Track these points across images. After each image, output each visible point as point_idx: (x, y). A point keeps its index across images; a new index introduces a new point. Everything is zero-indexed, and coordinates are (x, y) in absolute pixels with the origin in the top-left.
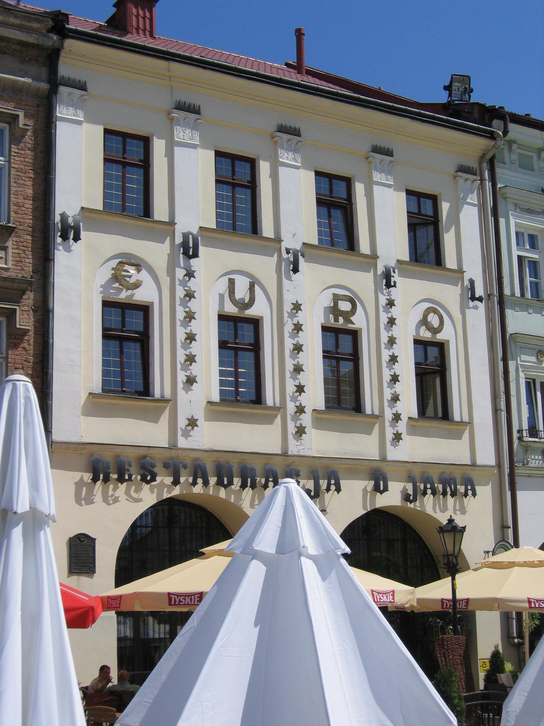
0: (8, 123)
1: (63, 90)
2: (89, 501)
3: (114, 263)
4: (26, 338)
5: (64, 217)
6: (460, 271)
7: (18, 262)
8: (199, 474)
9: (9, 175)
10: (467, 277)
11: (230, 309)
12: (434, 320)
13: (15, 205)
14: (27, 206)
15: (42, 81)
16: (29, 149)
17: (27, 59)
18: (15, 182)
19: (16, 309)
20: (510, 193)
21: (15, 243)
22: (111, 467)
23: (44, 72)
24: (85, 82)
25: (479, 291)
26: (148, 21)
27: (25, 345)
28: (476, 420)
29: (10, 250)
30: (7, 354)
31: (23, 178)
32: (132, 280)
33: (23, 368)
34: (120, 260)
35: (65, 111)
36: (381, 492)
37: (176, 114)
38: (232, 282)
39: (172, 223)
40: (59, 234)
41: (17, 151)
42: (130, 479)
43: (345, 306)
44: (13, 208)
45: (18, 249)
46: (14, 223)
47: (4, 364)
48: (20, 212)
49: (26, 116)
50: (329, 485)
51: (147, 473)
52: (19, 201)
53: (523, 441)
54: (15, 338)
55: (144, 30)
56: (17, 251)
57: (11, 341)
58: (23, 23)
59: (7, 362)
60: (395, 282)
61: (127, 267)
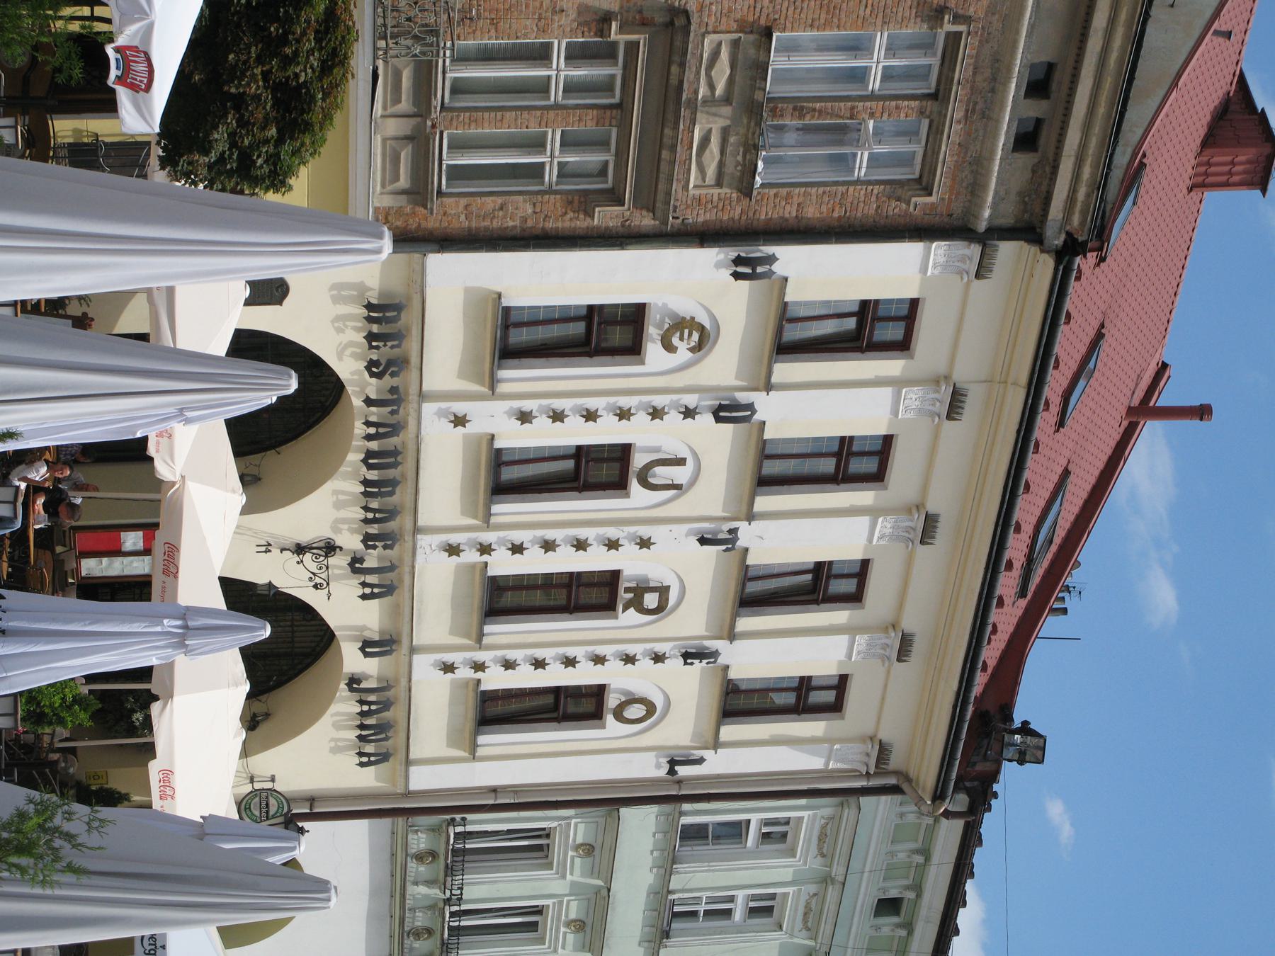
1: (976, 250)
2: (336, 300)
4: (582, 216)
5: (771, 259)
6: (716, 745)
7: (699, 201)
8: (381, 430)
10: (708, 754)
11: (638, 461)
12: (636, 711)
13: (788, 194)
14: (788, 207)
16: (878, 207)
17: (1026, 199)
18: (824, 193)
19: (623, 205)
20: (849, 814)
21: (728, 195)
23: (1007, 221)
25: (682, 771)
26: (1223, 179)
27: (571, 215)
28: (478, 765)
29: (716, 191)
30: (556, 192)
31: (832, 202)
32: (675, 340)
33: (535, 213)
34: (707, 325)
35: (941, 252)
36: (362, 649)
37: (945, 393)
38: (681, 462)
39: (769, 387)
40: (743, 255)
41: (875, 191)
42: (371, 347)
43: (651, 600)
44: (784, 191)
45: (719, 199)
46: (759, 193)
48: (777, 200)
49: (933, 204)
50: (371, 586)
51: (381, 368)
52: (795, 198)
53: (449, 825)
54: (580, 202)
55: (1206, 174)
56: (715, 198)
57: (576, 198)
60: (692, 664)
61: (696, 336)
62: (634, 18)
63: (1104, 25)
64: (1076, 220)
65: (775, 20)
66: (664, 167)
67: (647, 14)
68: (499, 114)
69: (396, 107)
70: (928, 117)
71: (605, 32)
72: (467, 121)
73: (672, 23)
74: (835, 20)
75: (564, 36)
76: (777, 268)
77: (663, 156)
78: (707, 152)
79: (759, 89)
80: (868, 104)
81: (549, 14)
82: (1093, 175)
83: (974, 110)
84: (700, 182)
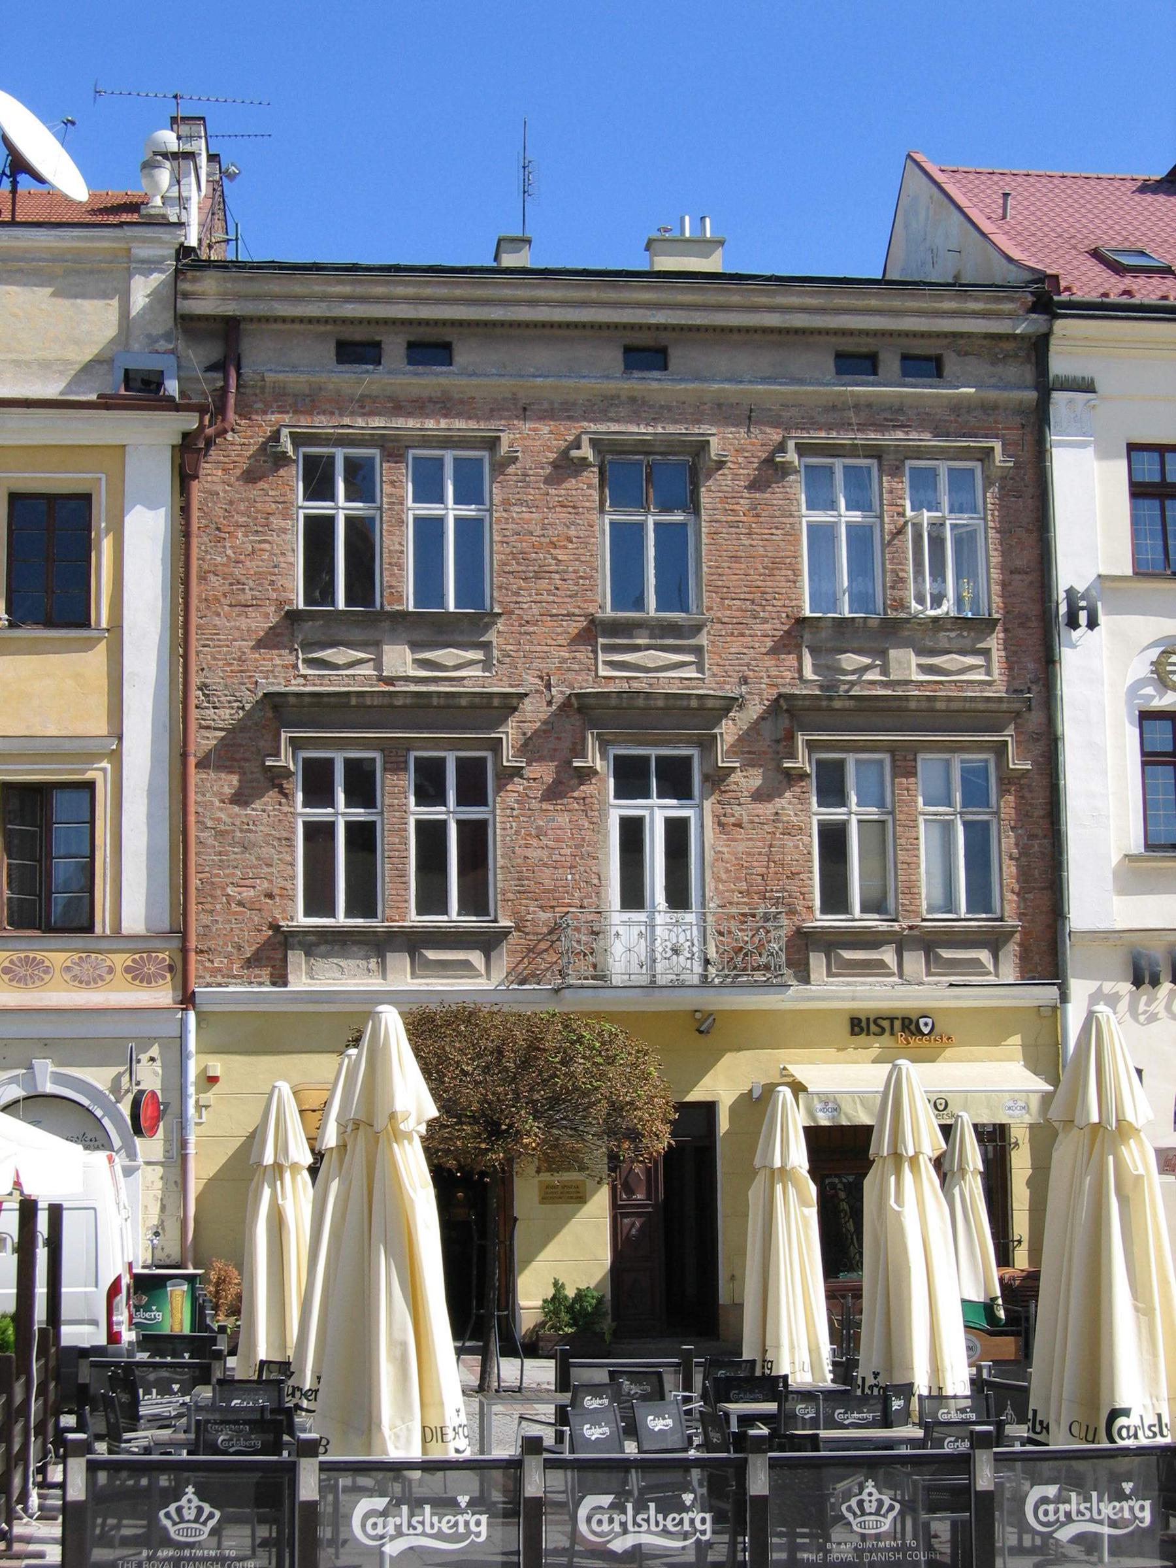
0: (979, 460)
1: (1059, 398)
3: (1154, 654)
5: (1070, 592)
9: (986, 538)
15: (1026, 388)
22: (1161, 963)
23: (1028, 373)
24: (1092, 379)
34: (1162, 648)
47: (995, 821)
58: (988, 306)
59: (999, 819)
62: (785, 747)
63: (778, 315)
64: (1007, 306)
65: (787, 616)
66: (955, 705)
67: (781, 734)
68: (899, 866)
69: (891, 965)
70: (903, 462)
71: (800, 772)
72: (908, 896)
73: (787, 711)
74: (788, 560)
75: (808, 810)
76: (1081, 588)
77: (943, 708)
78: (944, 666)
79: (865, 623)
80: (886, 520)
81: (780, 825)
82: (951, 299)
83: (892, 420)
84: (982, 670)
